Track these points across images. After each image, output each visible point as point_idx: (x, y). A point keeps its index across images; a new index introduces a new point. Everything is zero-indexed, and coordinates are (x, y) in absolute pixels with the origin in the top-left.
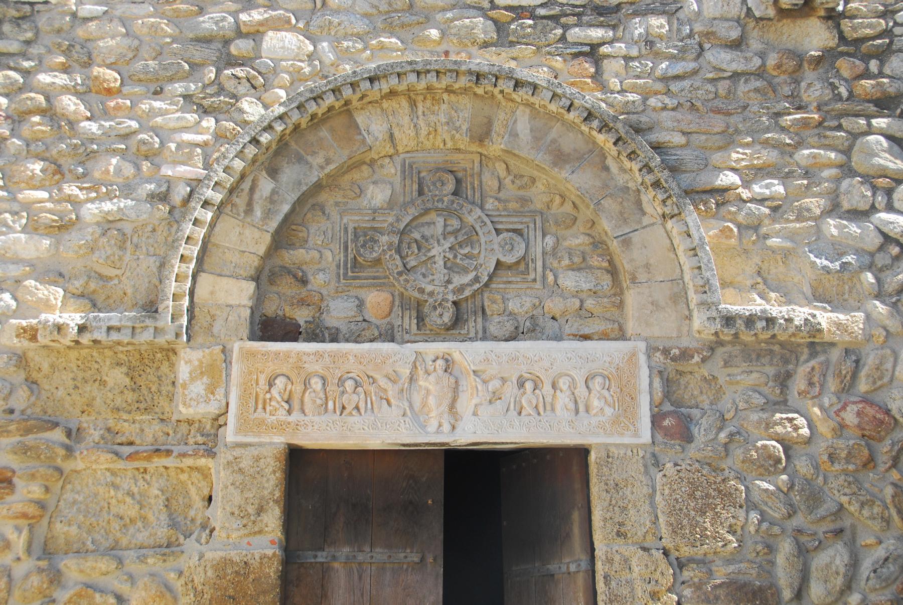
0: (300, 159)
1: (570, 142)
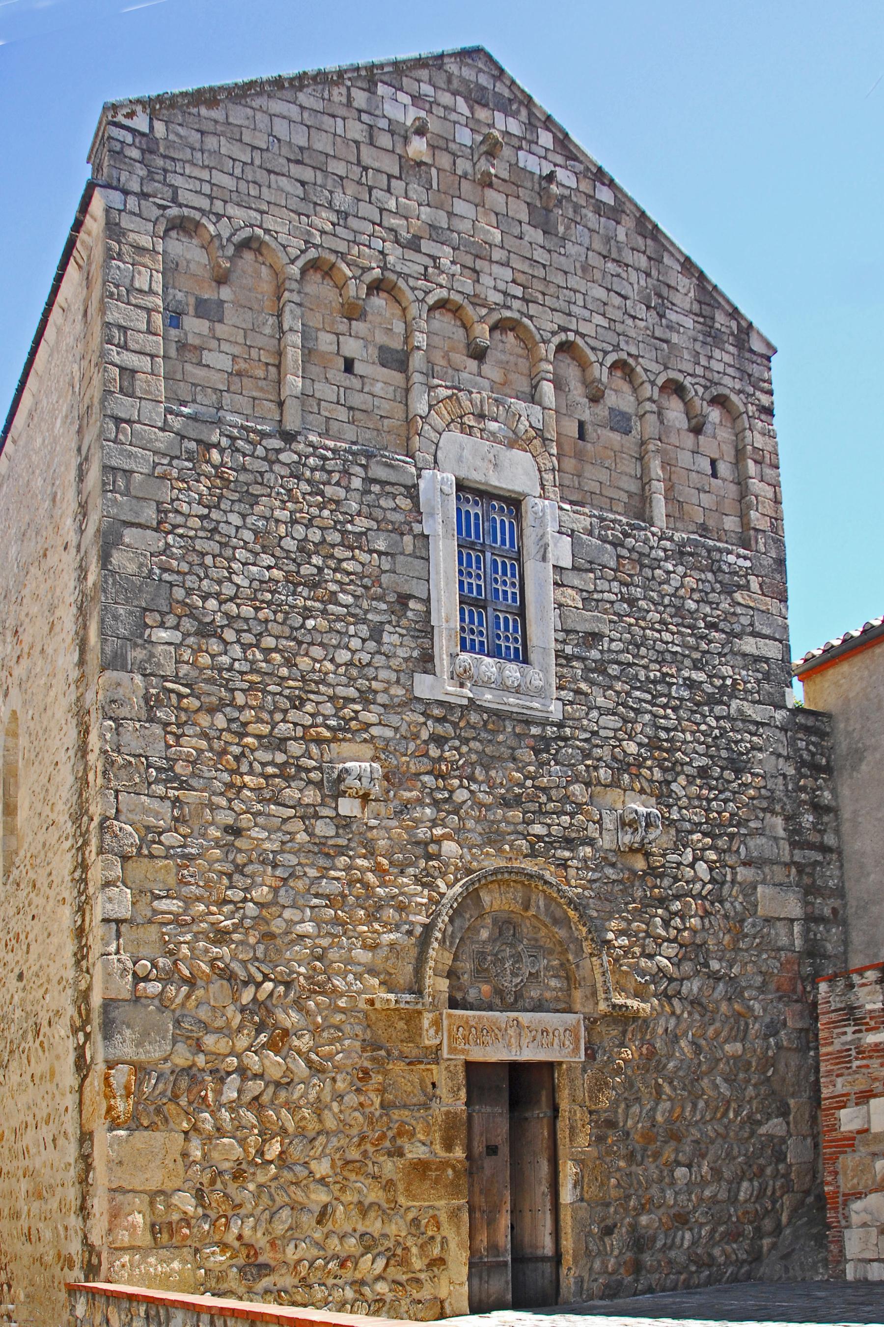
1: (558, 913)
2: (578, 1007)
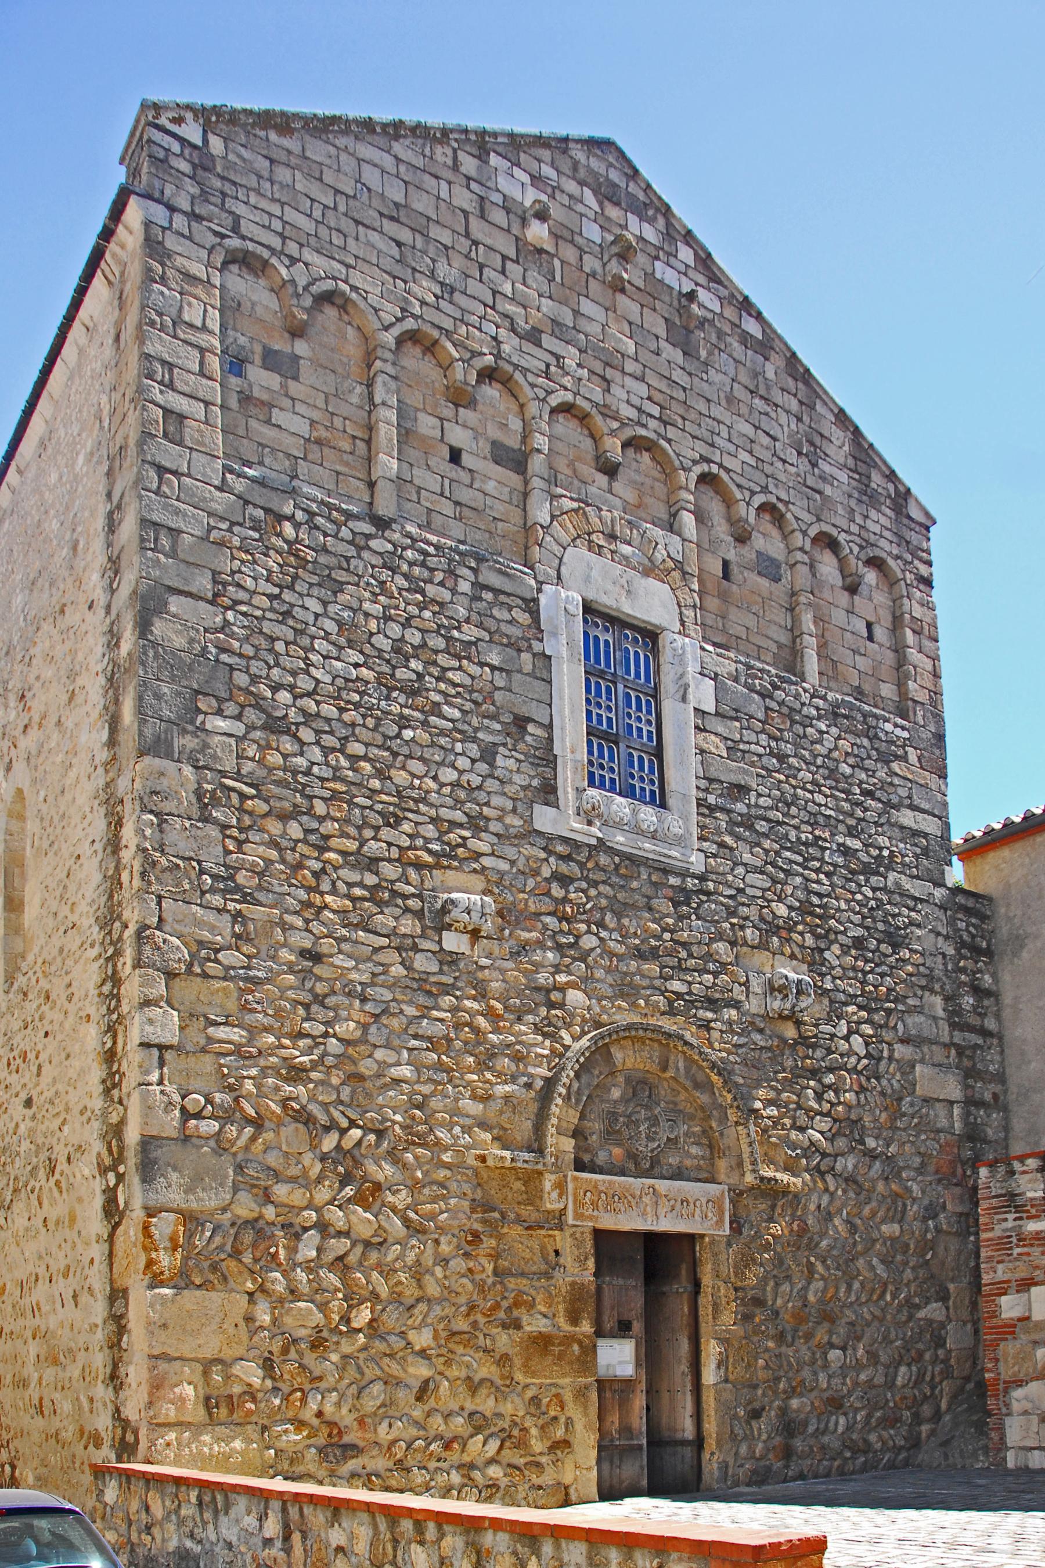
1: (700, 1077)
2: (722, 1177)
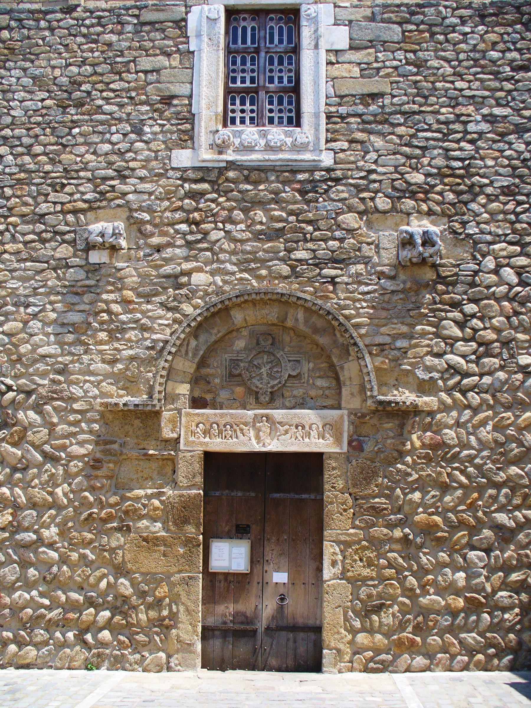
0: (207, 331)
